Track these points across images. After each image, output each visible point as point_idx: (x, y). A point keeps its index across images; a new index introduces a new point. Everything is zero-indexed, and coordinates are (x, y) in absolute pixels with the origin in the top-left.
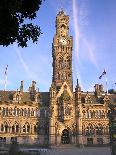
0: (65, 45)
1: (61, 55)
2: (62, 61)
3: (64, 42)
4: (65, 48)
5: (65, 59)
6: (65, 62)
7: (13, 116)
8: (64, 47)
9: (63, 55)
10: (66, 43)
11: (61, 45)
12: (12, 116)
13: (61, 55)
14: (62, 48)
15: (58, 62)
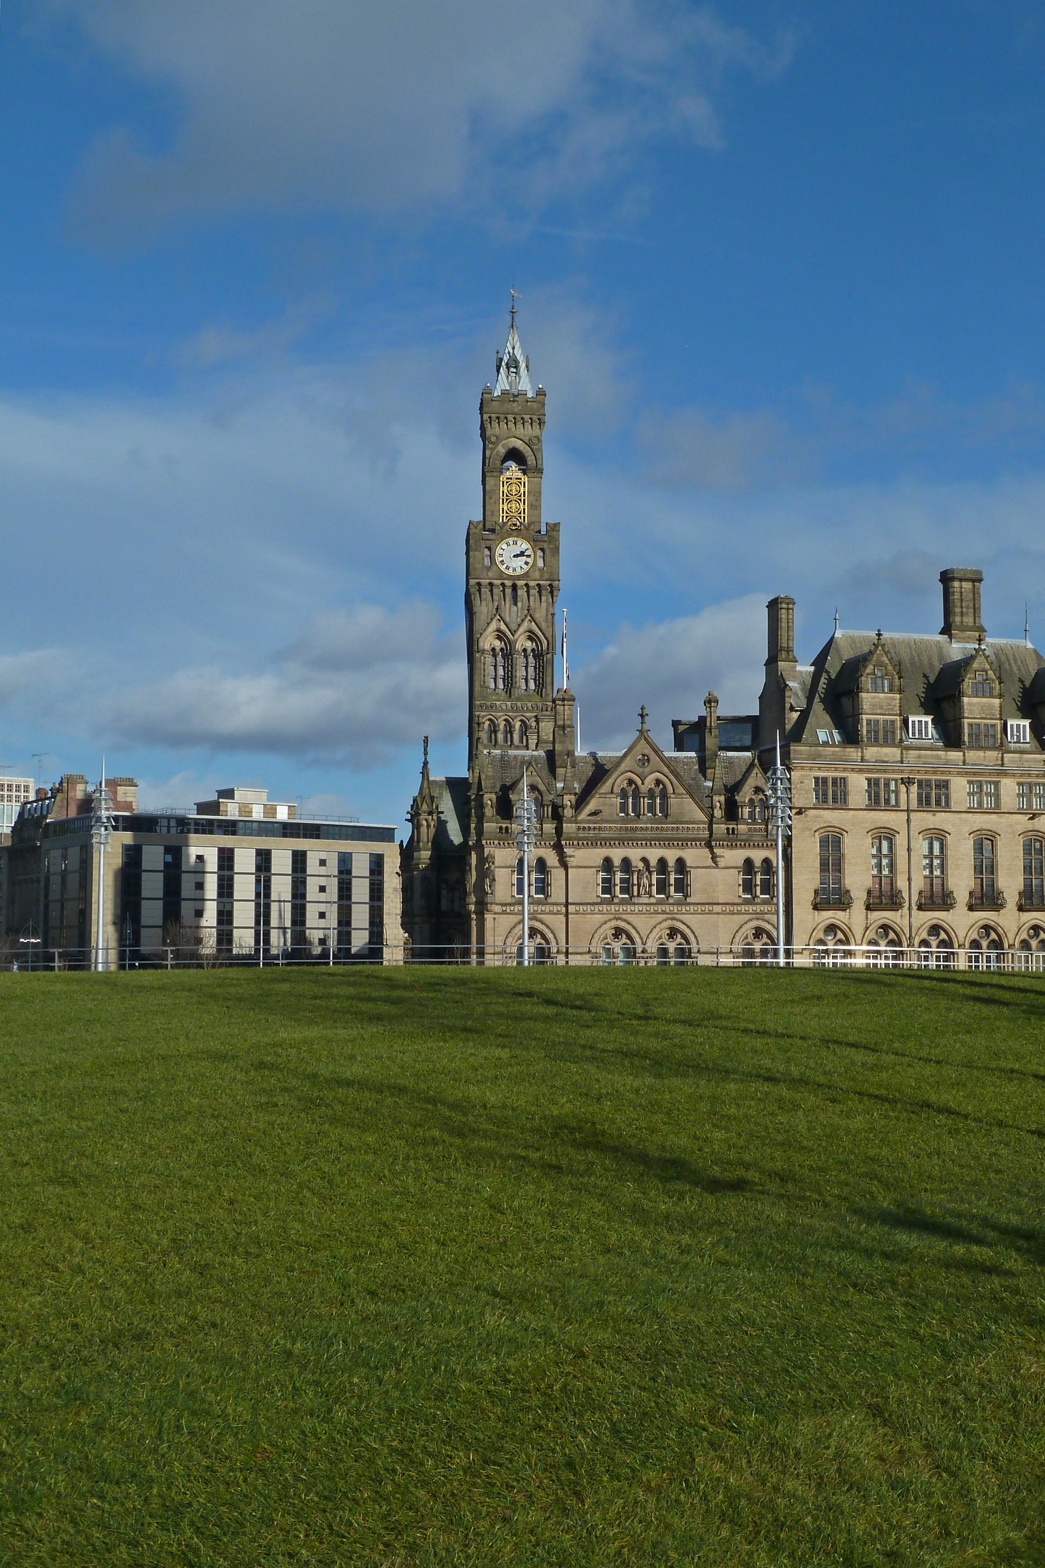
0: (519, 578)
1: (503, 627)
2: (508, 654)
3: (512, 557)
4: (522, 593)
5: (522, 643)
6: (520, 660)
7: (660, 903)
8: (514, 587)
9: (513, 627)
10: (526, 563)
11: (501, 575)
12: (652, 900)
13: (503, 627)
14: (509, 591)
15: (489, 659)
